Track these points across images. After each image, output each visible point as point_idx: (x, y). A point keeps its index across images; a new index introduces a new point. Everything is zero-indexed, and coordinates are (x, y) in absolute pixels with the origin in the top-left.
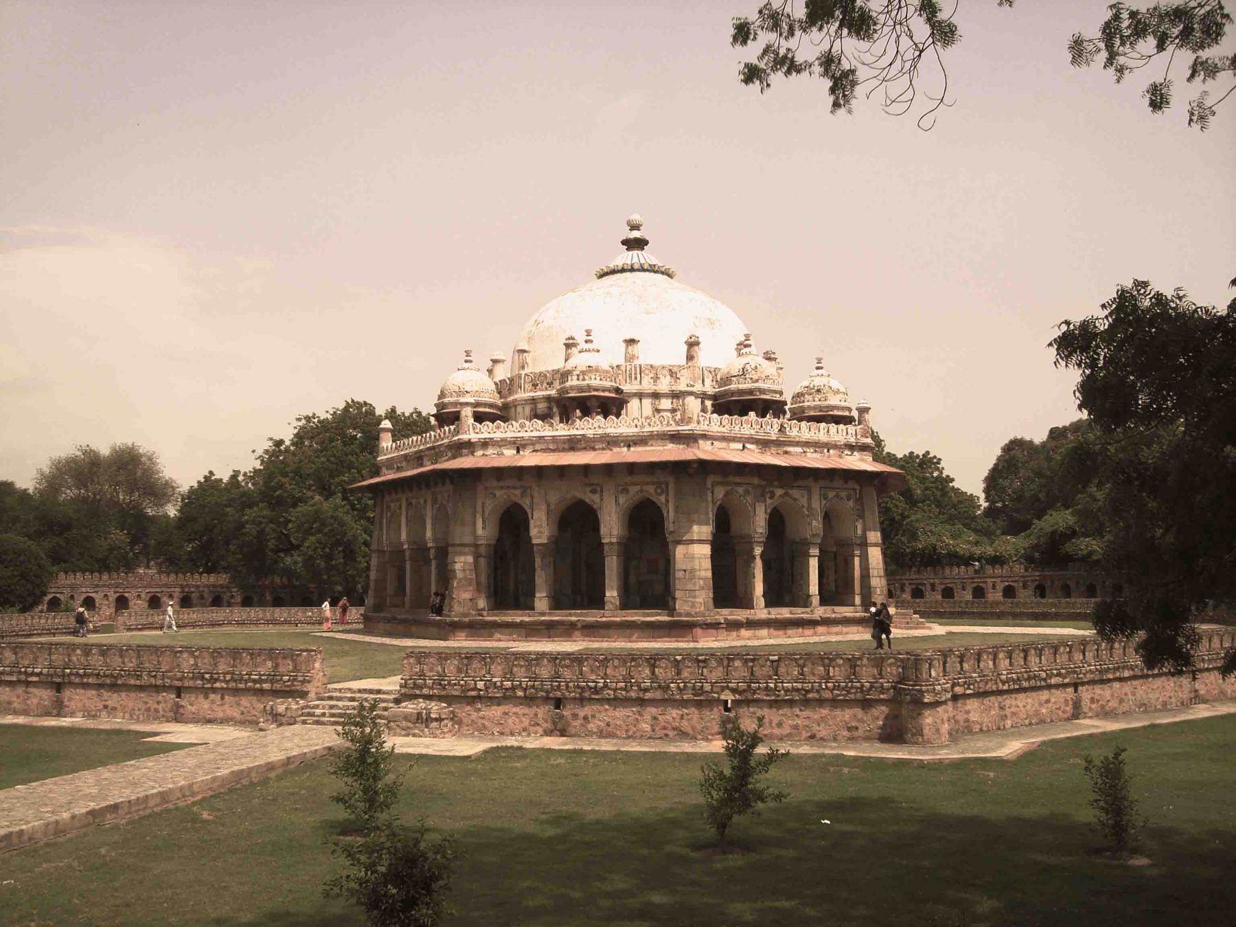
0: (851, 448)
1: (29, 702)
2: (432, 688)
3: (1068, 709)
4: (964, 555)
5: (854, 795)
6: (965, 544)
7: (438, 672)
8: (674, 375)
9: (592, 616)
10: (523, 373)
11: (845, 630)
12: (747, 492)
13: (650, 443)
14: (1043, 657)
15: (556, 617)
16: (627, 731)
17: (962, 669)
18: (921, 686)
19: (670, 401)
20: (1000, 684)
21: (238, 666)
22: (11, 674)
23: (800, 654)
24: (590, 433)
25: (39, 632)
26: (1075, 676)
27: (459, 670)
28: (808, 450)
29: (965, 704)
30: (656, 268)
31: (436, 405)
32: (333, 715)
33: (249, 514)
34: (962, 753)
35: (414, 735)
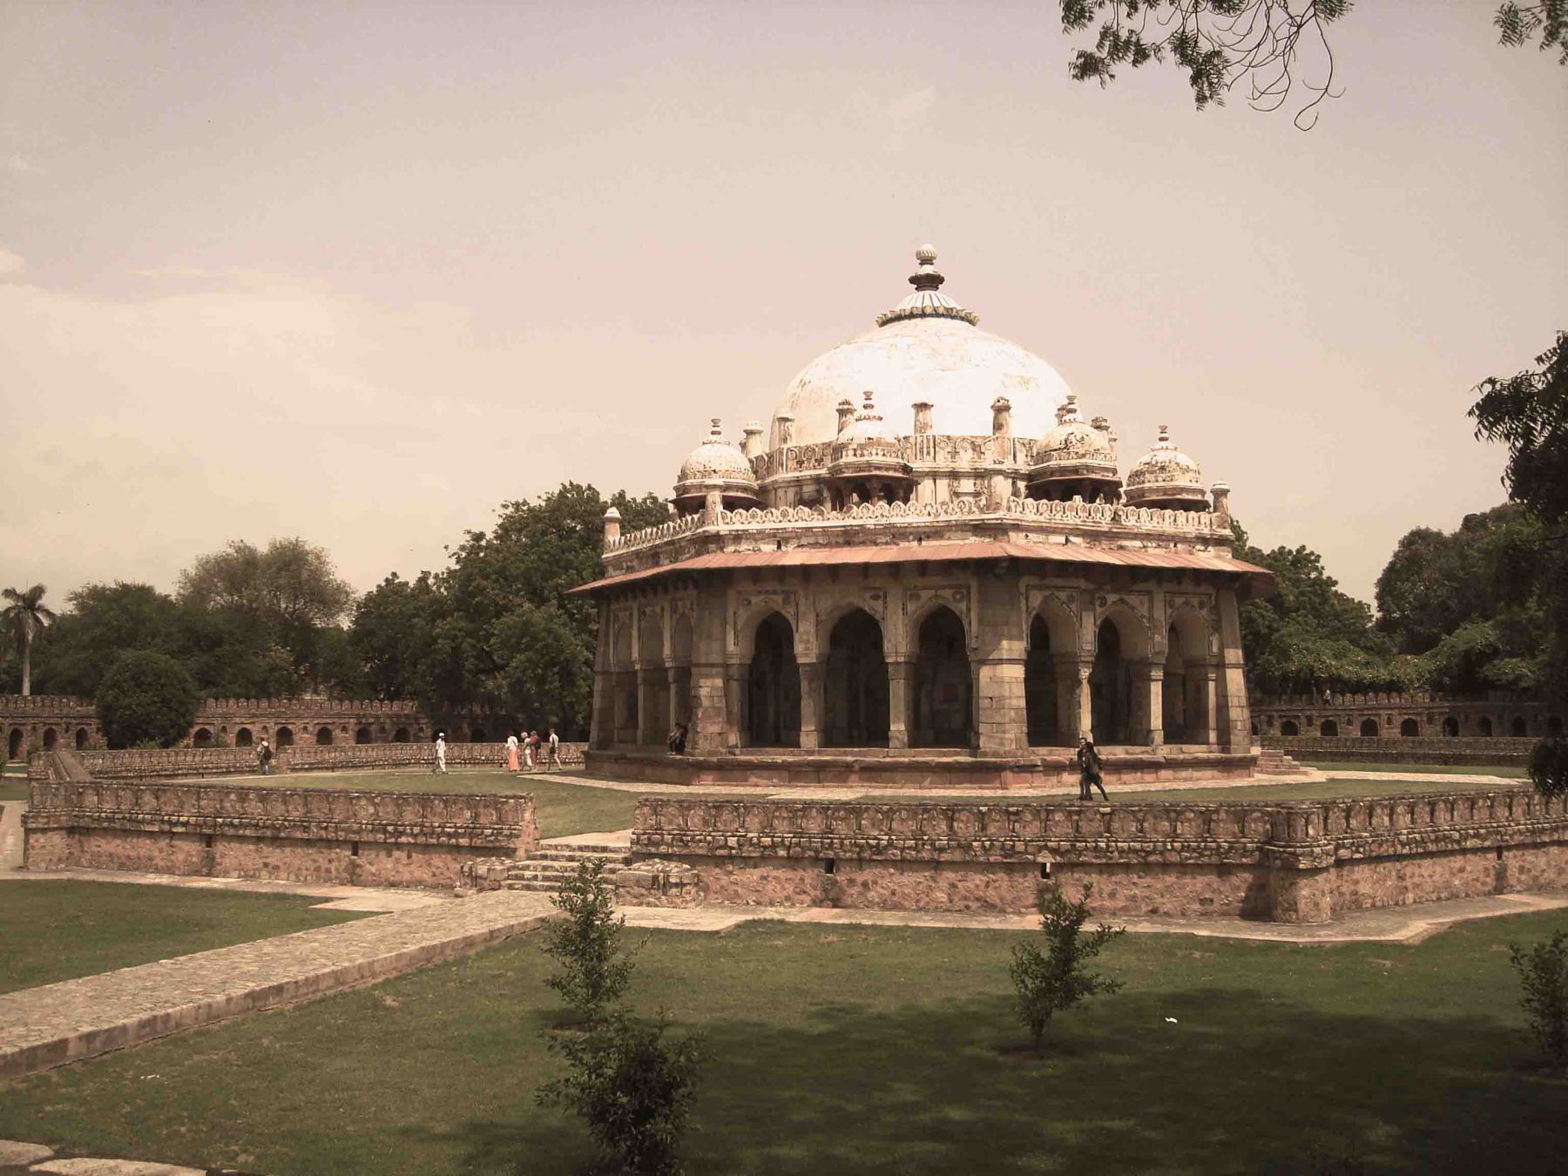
0: (1205, 541)
1: (172, 858)
2: (672, 845)
3: (1488, 880)
4: (1350, 679)
5: (1208, 987)
6: (1352, 666)
7: (679, 825)
8: (978, 449)
9: (874, 756)
10: (785, 447)
11: (1196, 774)
12: (1071, 599)
13: (946, 536)
14: (1455, 813)
15: (827, 757)
16: (918, 901)
17: (1348, 826)
18: (1295, 847)
19: (972, 481)
20: (1399, 847)
21: (429, 816)
22: (151, 822)
23: (1140, 805)
24: (870, 523)
25: (185, 771)
26: (1499, 837)
27: (706, 823)
28: (1149, 544)
29: (1353, 872)
30: (954, 313)
31: (676, 489)
32: (546, 878)
33: (441, 627)
34: (1348, 934)
35: (649, 904)
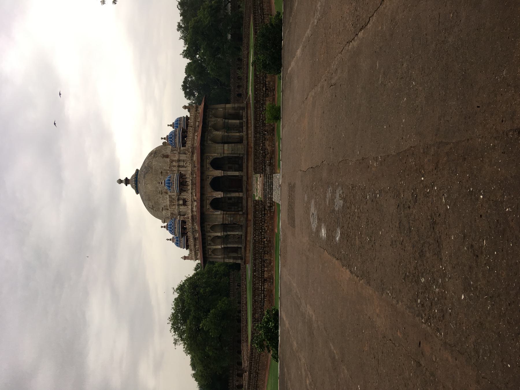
9: (245, 178)
12: (209, 136)
